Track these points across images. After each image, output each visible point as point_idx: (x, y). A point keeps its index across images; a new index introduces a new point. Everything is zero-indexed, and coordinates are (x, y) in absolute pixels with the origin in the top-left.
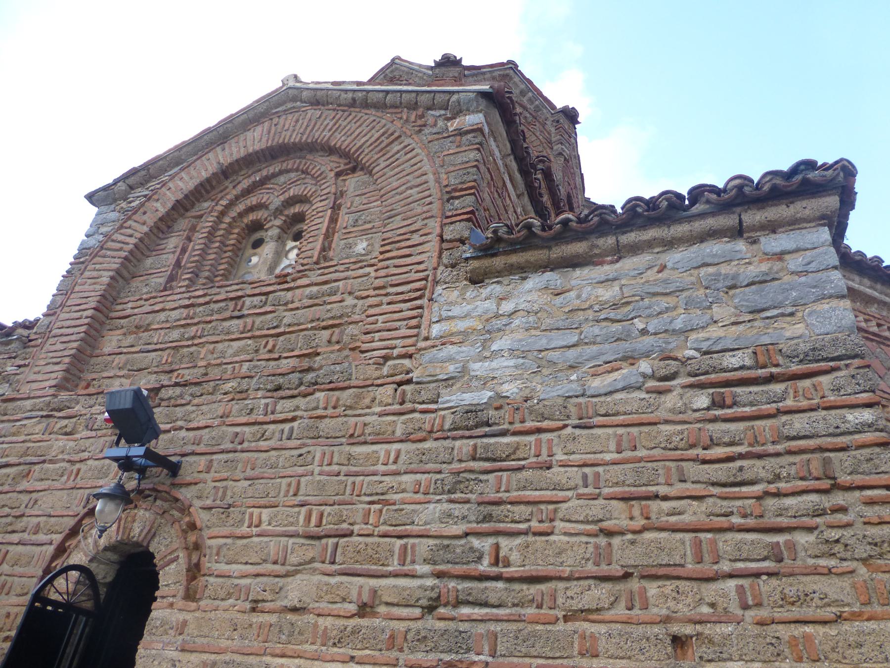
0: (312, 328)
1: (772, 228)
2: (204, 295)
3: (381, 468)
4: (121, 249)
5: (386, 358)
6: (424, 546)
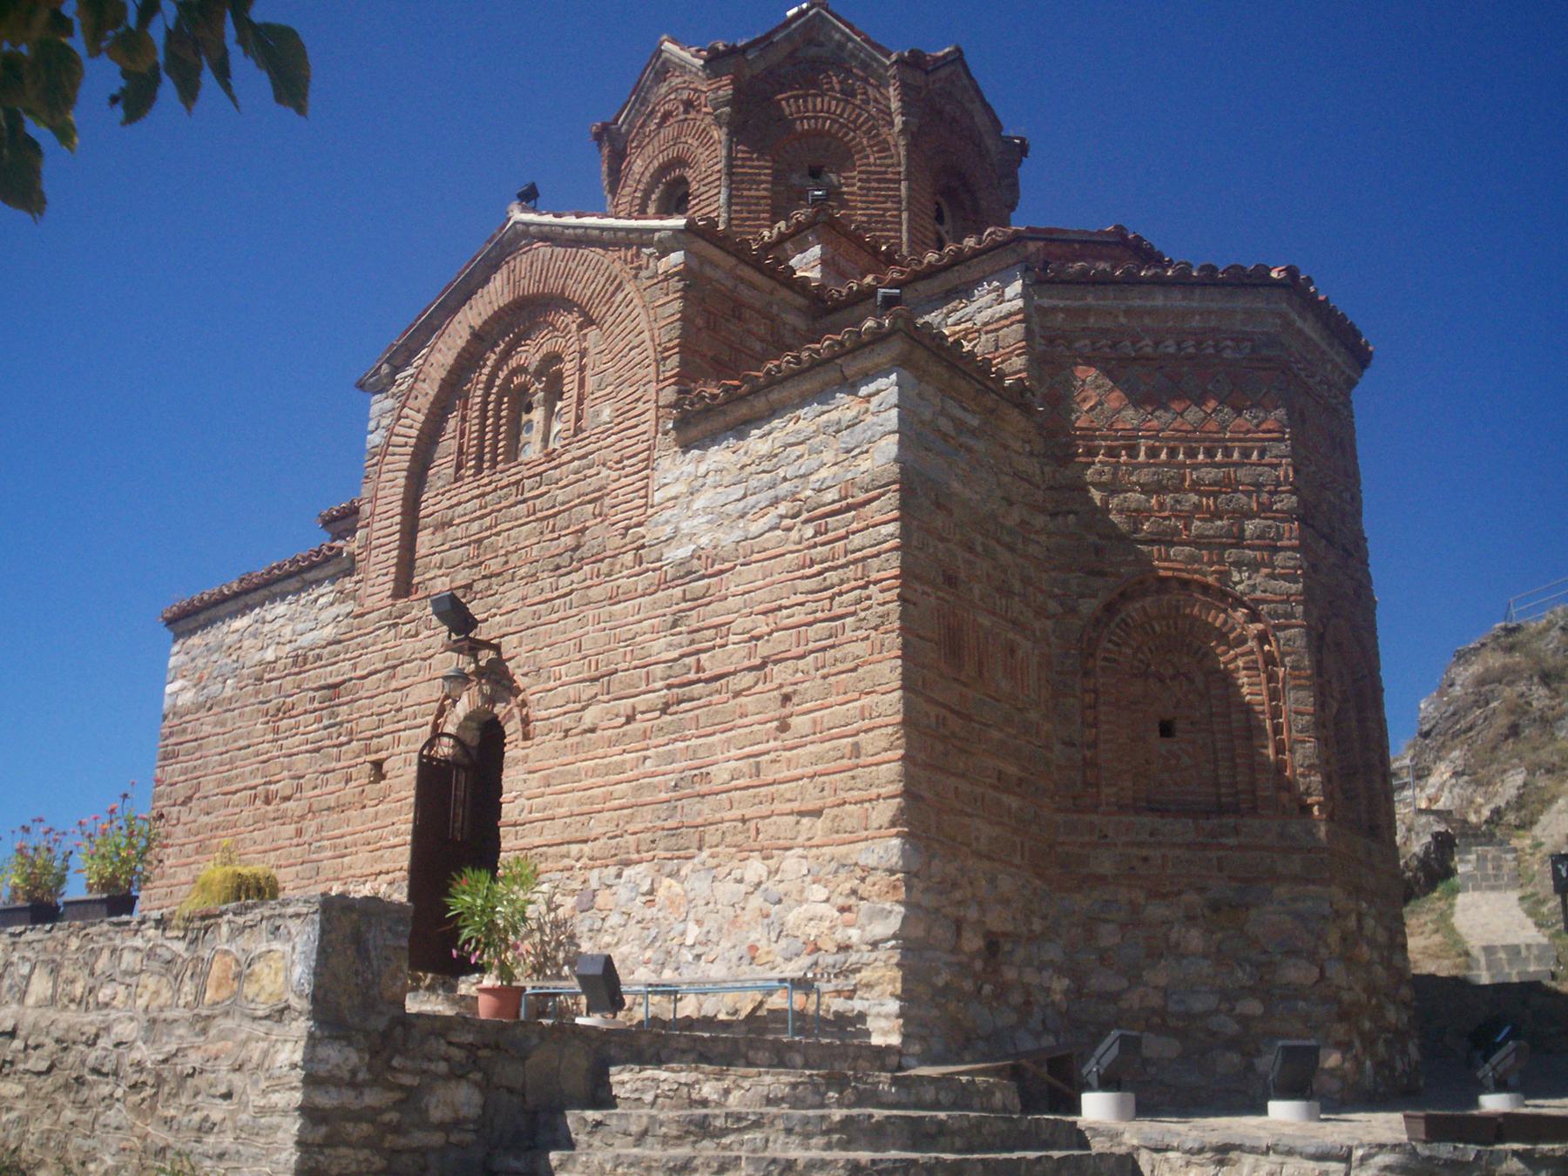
0: (581, 504)
2: (490, 483)
3: (631, 619)
4: (406, 445)
5: (627, 528)
6: (658, 670)
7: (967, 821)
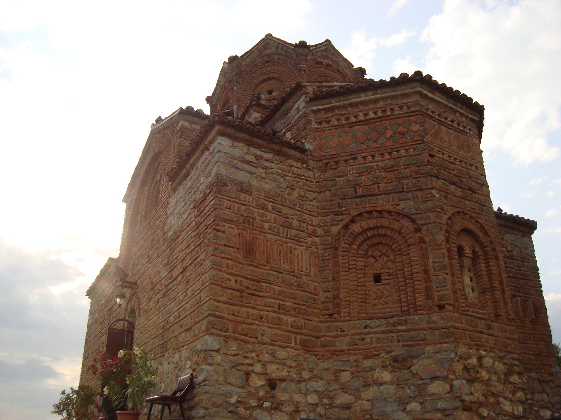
1: (211, 143)
7: (255, 327)
